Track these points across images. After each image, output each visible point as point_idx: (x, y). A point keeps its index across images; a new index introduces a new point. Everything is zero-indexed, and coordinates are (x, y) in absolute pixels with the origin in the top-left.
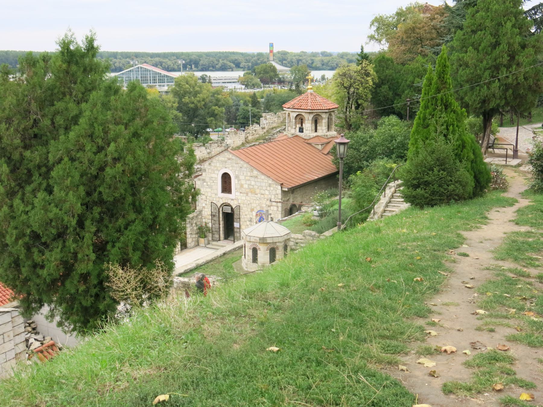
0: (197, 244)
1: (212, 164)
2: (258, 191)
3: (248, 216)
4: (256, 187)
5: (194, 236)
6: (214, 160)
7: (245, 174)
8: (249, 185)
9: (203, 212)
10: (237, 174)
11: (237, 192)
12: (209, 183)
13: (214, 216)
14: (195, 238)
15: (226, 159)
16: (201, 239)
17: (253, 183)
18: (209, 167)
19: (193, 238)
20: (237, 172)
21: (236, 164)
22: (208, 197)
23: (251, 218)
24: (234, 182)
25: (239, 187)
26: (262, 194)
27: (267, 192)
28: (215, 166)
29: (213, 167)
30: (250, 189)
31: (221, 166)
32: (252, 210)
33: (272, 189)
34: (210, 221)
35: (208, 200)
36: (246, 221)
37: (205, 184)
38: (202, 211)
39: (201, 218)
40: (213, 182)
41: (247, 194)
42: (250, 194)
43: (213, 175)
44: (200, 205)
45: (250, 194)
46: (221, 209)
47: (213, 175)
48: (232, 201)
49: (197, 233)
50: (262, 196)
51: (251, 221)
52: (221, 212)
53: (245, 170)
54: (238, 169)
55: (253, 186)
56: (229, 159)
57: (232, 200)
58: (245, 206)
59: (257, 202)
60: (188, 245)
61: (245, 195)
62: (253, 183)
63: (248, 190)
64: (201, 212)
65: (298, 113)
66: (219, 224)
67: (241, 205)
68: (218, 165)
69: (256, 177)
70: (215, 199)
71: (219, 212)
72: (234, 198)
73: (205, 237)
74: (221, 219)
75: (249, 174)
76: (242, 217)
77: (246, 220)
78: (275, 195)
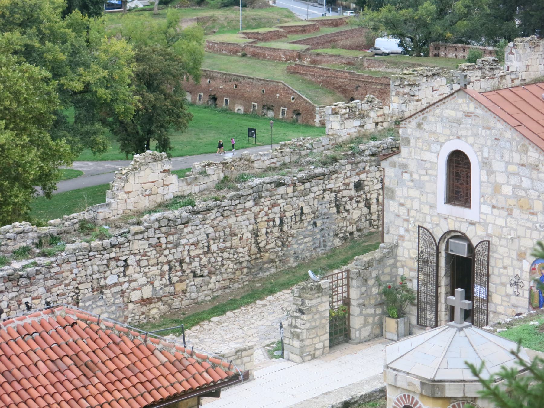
0: (378, 331)
1: (425, 126)
3: (511, 272)
4: (533, 194)
5: (371, 311)
6: (430, 116)
7: (506, 158)
8: (515, 187)
9: (400, 251)
10: (486, 155)
11: (485, 203)
12: (416, 176)
13: (426, 262)
14: (375, 315)
15: (460, 115)
16: (388, 319)
17: (526, 183)
18: (417, 134)
19: (367, 316)
20: (486, 150)
21: (484, 128)
22: (413, 213)
23: (518, 277)
25: (489, 190)
28: (432, 133)
29: (426, 135)
30: (519, 198)
31: (448, 132)
32: (521, 256)
34: (415, 274)
35: (412, 220)
36: (504, 285)
37: (406, 176)
38: (396, 246)
39: (394, 266)
40: (427, 174)
41: (510, 212)
42: (516, 212)
43: (427, 156)
44: (392, 231)
45: (516, 212)
46: (443, 247)
47: (427, 156)
48: (472, 228)
49: (381, 304)
51: (516, 285)
52: (443, 254)
53: (508, 145)
54: (489, 143)
55: (526, 190)
56: (468, 115)
57: (472, 224)
58: (503, 242)
60: (354, 334)
61: (504, 213)
62: (526, 183)
63: (512, 202)
64: (393, 248)
66: (437, 286)
67: (494, 241)
70: (428, 219)
71: (438, 252)
72: (476, 219)
73: (401, 314)
74: (442, 272)
75: (517, 158)
76: (494, 271)
77: (504, 279)
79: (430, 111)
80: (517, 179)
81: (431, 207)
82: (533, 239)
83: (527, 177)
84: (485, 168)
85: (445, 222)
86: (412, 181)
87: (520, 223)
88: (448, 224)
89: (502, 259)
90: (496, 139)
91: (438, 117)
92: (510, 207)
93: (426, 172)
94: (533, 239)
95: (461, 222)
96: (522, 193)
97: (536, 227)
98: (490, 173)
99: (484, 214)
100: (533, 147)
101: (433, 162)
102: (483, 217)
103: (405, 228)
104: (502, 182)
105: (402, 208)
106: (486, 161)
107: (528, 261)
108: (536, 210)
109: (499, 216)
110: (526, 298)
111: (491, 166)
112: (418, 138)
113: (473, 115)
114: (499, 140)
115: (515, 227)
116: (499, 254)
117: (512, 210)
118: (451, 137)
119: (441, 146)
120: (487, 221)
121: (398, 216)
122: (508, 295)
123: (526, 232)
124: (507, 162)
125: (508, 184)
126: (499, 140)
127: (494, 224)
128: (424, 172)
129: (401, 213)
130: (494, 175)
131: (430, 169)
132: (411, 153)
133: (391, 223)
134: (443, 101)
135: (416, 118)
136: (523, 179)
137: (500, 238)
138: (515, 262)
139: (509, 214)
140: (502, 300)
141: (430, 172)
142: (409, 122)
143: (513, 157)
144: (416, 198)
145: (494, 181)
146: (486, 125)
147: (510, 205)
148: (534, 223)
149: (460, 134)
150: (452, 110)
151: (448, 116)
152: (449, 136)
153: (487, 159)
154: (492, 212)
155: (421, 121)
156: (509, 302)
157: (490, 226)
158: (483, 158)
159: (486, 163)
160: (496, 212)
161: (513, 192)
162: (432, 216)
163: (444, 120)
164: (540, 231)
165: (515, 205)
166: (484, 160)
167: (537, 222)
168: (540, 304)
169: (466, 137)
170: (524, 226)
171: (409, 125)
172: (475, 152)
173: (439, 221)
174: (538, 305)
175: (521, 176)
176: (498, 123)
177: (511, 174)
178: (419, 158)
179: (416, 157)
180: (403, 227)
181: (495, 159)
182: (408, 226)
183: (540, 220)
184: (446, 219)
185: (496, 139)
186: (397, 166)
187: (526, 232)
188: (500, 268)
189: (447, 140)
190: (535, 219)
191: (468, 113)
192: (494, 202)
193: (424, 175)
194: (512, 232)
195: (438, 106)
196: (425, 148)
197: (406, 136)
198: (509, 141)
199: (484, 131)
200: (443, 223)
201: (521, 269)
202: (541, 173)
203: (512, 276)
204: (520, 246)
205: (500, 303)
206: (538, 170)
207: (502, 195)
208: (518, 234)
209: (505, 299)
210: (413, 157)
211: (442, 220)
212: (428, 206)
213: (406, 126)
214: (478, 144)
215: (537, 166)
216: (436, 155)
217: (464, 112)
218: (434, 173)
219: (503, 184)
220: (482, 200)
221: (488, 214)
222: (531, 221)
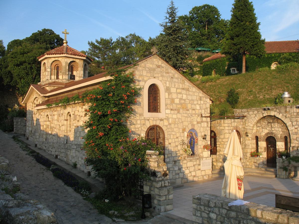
2: (189, 106)
3: (180, 139)
4: (187, 101)
7: (177, 86)
10: (168, 85)
11: (167, 109)
15: (154, 66)
17: (185, 97)
20: (168, 83)
24: (163, 96)
25: (169, 102)
26: (193, 110)
27: (198, 107)
30: (181, 104)
31: (149, 75)
32: (184, 130)
33: (202, 102)
42: (181, 111)
50: (194, 112)
53: (176, 80)
54: (169, 79)
55: (185, 100)
56: (159, 67)
57: (161, 120)
58: (176, 126)
59: (189, 119)
61: (176, 112)
63: (179, 106)
65: (71, 60)
68: (145, 73)
69: (188, 90)
78: (205, 109)
80: (182, 95)
81: (140, 115)
82: (187, 121)
84: (168, 91)
85: (148, 122)
87: (183, 115)
88: (150, 122)
89: (176, 134)
90: (172, 78)
91: (144, 67)
96: (183, 102)
98: (170, 93)
99: (167, 114)
100: (186, 81)
102: (167, 115)
104: (174, 98)
106: (168, 88)
107: (186, 132)
109: (174, 114)
111: (170, 90)
114: (173, 78)
115: (181, 118)
116: (175, 132)
117: (179, 110)
118: (151, 78)
119: (145, 82)
120: (169, 117)
125: (177, 98)
126: (173, 78)
134: (146, 60)
136: (183, 95)
138: (181, 134)
143: (179, 86)
145: (171, 98)
146: (166, 71)
148: (188, 114)
149: (155, 76)
151: (148, 67)
152: (150, 77)
153: (168, 87)
154: (171, 112)
157: (170, 119)
160: (172, 112)
161: (179, 102)
162: (140, 120)
163: (147, 69)
164: (191, 117)
169: (158, 77)
170: (184, 116)
172: (163, 84)
173: (145, 122)
175: (182, 94)
181: (172, 87)
183: (190, 113)
185: (172, 78)
188: (175, 139)
189: (148, 79)
190: (188, 112)
191: (159, 66)
192: (171, 107)
194: (180, 120)
195: (143, 62)
198: (177, 78)
199: (166, 74)
200: (147, 123)
201: (184, 137)
203: (180, 141)
204: (183, 126)
208: (182, 121)
219: (175, 98)
220: (166, 108)
222: (187, 114)
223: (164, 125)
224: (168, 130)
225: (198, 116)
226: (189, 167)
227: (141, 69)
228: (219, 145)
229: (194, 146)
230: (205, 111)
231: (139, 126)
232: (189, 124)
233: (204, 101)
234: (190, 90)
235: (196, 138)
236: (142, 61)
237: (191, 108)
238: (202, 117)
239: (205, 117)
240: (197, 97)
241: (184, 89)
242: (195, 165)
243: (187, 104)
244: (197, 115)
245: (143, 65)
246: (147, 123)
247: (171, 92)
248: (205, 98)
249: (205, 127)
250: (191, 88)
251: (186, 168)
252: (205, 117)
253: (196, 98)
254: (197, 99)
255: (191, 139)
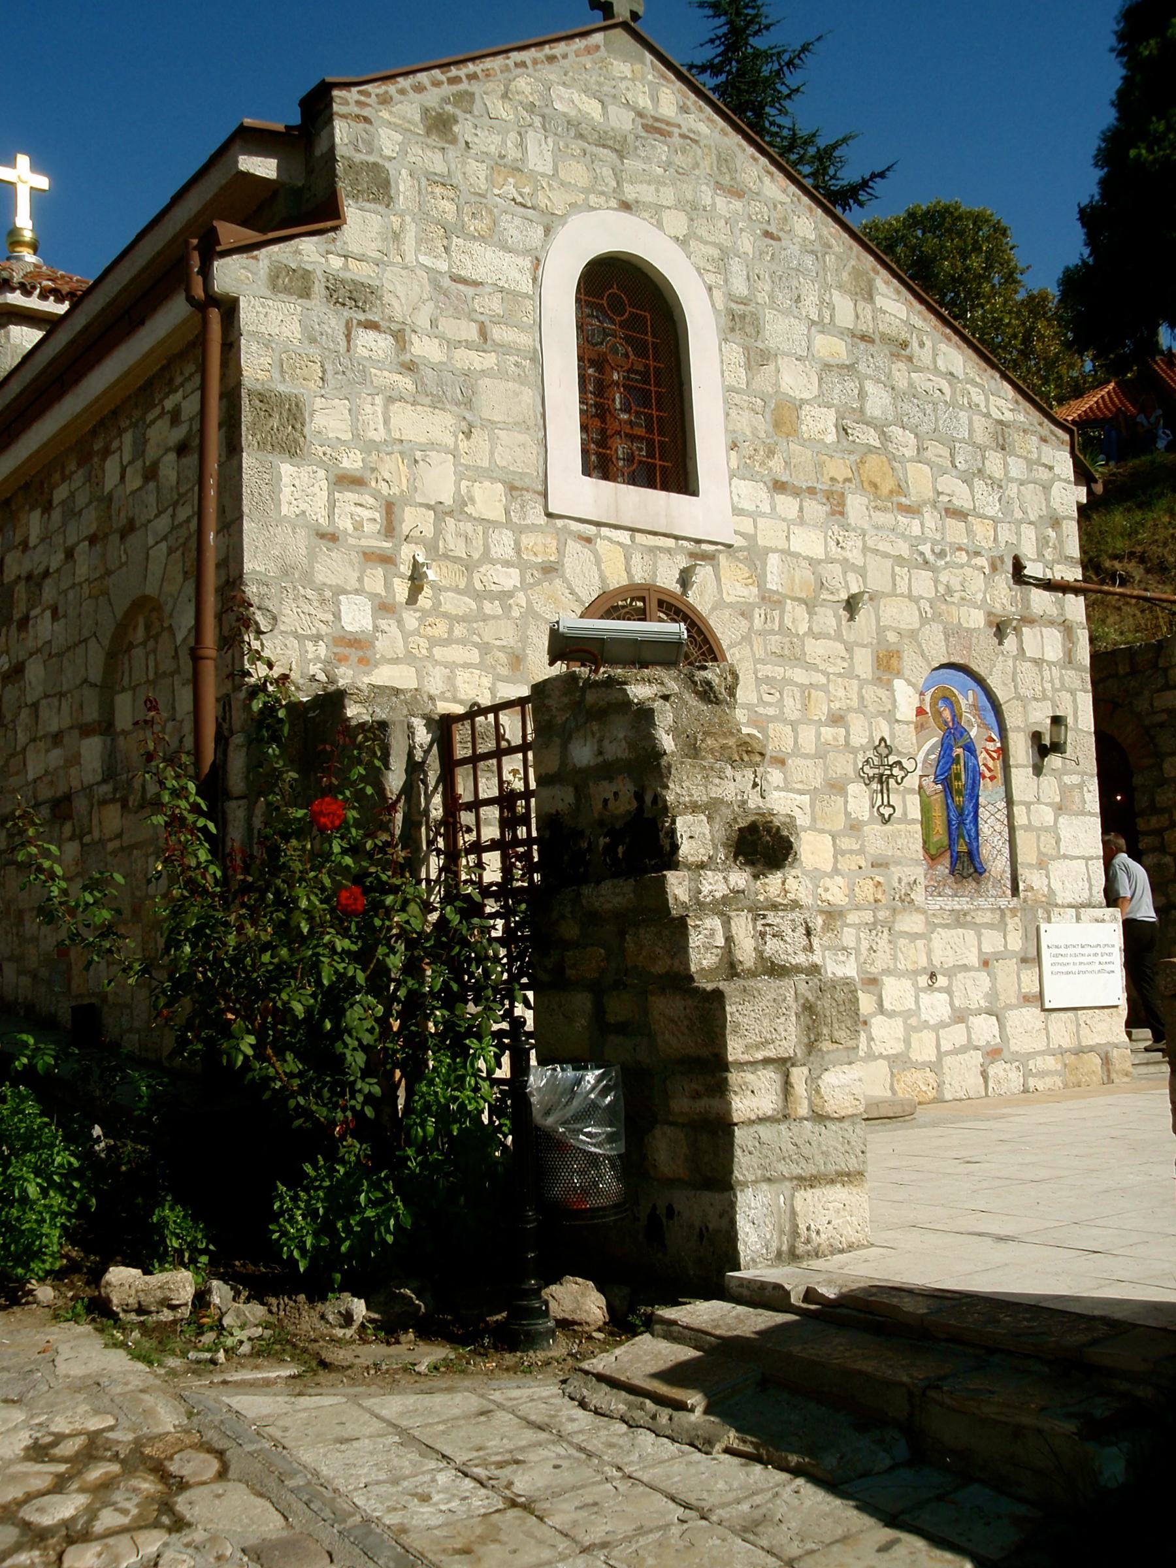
2: (919, 481)
4: (905, 441)
10: (740, 287)
12: (424, 348)
20: (737, 267)
22: (413, 519)
23: (884, 747)
28: (501, 166)
29: (477, 172)
31: (576, 173)
41: (837, 506)
42: (856, 504)
50: (955, 531)
59: (923, 583)
61: (816, 509)
63: (838, 468)
68: (539, 156)
69: (899, 348)
75: (845, 310)
79: (488, 74)
80: (852, 385)
81: (512, 488)
82: (916, 600)
83: (879, 381)
86: (410, 367)
87: (870, 543)
88: (598, 563)
90: (767, 234)
92: (838, 487)
93: (483, 333)
94: (916, 600)
95: (653, 550)
96: (871, 437)
97: (922, 554)
100: (887, 283)
101: (515, 294)
102: (746, 525)
103: (373, 596)
105: (347, 497)
108: (912, 500)
109: (801, 521)
110: (913, 821)
112: (435, 180)
113: (676, 131)
115: (859, 562)
118: (593, 200)
119: (548, 231)
121: (330, 537)
122: (854, 827)
123: (893, 575)
124: (813, 322)
127: (787, 553)
128: (470, 332)
129: (345, 524)
130: (772, 367)
131: (498, 320)
132: (396, 236)
133: (286, 572)
135: (419, 88)
136: (870, 386)
137: (810, 605)
138: (871, 692)
139: (833, 513)
140: (838, 853)
141: (498, 333)
142: (385, 100)
144: (433, 445)
147: (832, 479)
149: (630, 192)
150: (586, 91)
151: (573, 113)
153: (744, 302)
155: (449, 108)
156: (861, 852)
157: (773, 560)
158: (731, 297)
159: (743, 317)
160: (787, 505)
162: (519, 530)
165: (848, 480)
166: (734, 306)
167: (922, 539)
168: (950, 834)
169: (658, 209)
170: (886, 555)
171: (385, 114)
173: (560, 551)
174: (946, 842)
176: (767, 180)
177: (827, 367)
178: (443, 266)
179: (423, 259)
180: (357, 592)
182: (388, 585)
184: (588, 540)
185: (767, 234)
186: (318, 289)
187: (893, 575)
191: (657, 120)
192: (776, 464)
193: (469, 346)
195: (523, 64)
196: (473, 226)
197: (371, 159)
199: (721, 202)
200: (576, 558)
202: (918, 370)
204: (881, 630)
205: (828, 868)
206: (910, 359)
207: (804, 443)
209: (846, 843)
210: (410, 258)
211: (573, 546)
212: (499, 487)
213: (365, 112)
214: (706, 243)
215: (905, 345)
216: (527, 263)
217: (640, 114)
218: (524, 340)
221: (763, 515)
223: (720, 605)
224: (757, 642)
225: (994, 568)
226: (950, 973)
227: (501, 110)
228: (1159, 832)
229: (976, 806)
230: (1043, 542)
231: (509, 579)
232: (924, 620)
233: (1030, 463)
234: (923, 356)
235: (991, 746)
236: (516, 56)
237: (931, 495)
238: (1018, 574)
239: (1049, 585)
240: (979, 422)
241: (872, 341)
242: (998, 956)
243: (903, 460)
244: (982, 561)
245: (523, 84)
246: (576, 558)
247: (772, 344)
248: (1035, 439)
249: (1051, 664)
250: (928, 344)
251: (923, 980)
252: (1049, 585)
253: (971, 431)
254: (981, 438)
255: (946, 747)
